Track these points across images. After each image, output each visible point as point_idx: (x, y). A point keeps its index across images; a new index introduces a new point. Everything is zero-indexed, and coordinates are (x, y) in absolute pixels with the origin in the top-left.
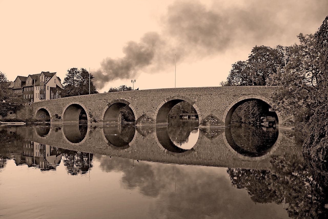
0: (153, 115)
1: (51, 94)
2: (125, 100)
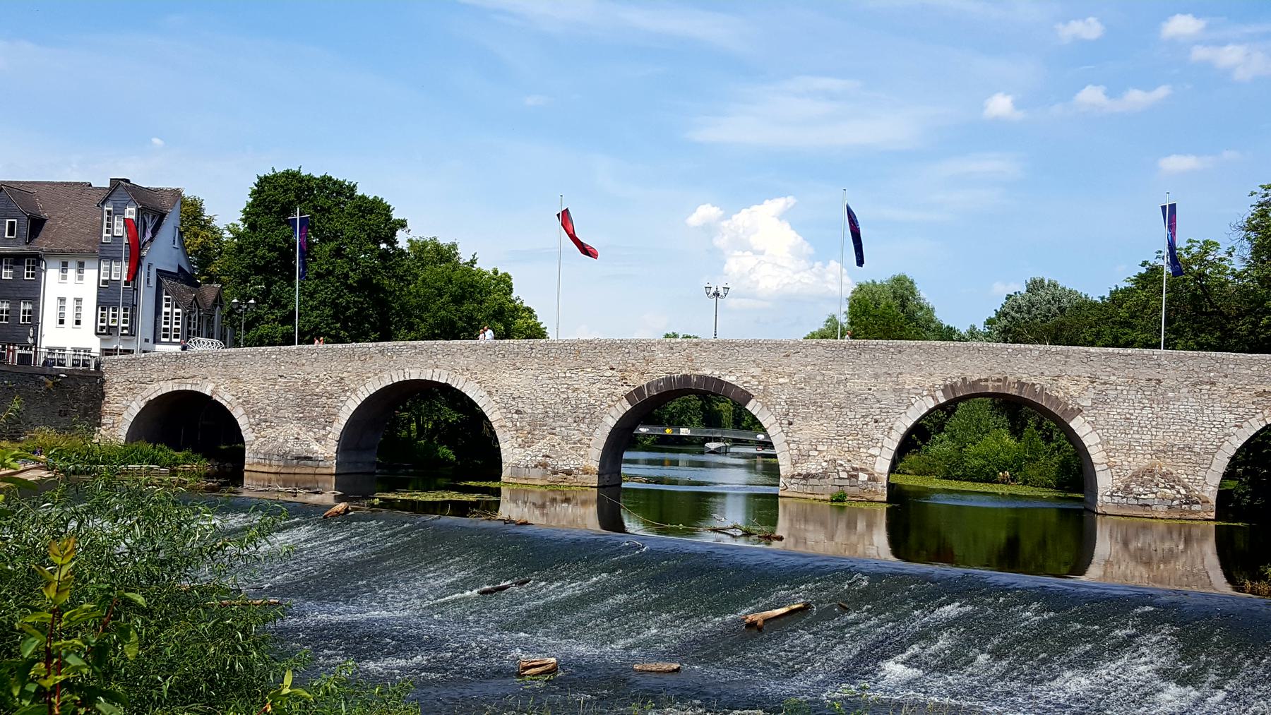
0: (871, 455)
1: (165, 309)
2: (727, 379)
